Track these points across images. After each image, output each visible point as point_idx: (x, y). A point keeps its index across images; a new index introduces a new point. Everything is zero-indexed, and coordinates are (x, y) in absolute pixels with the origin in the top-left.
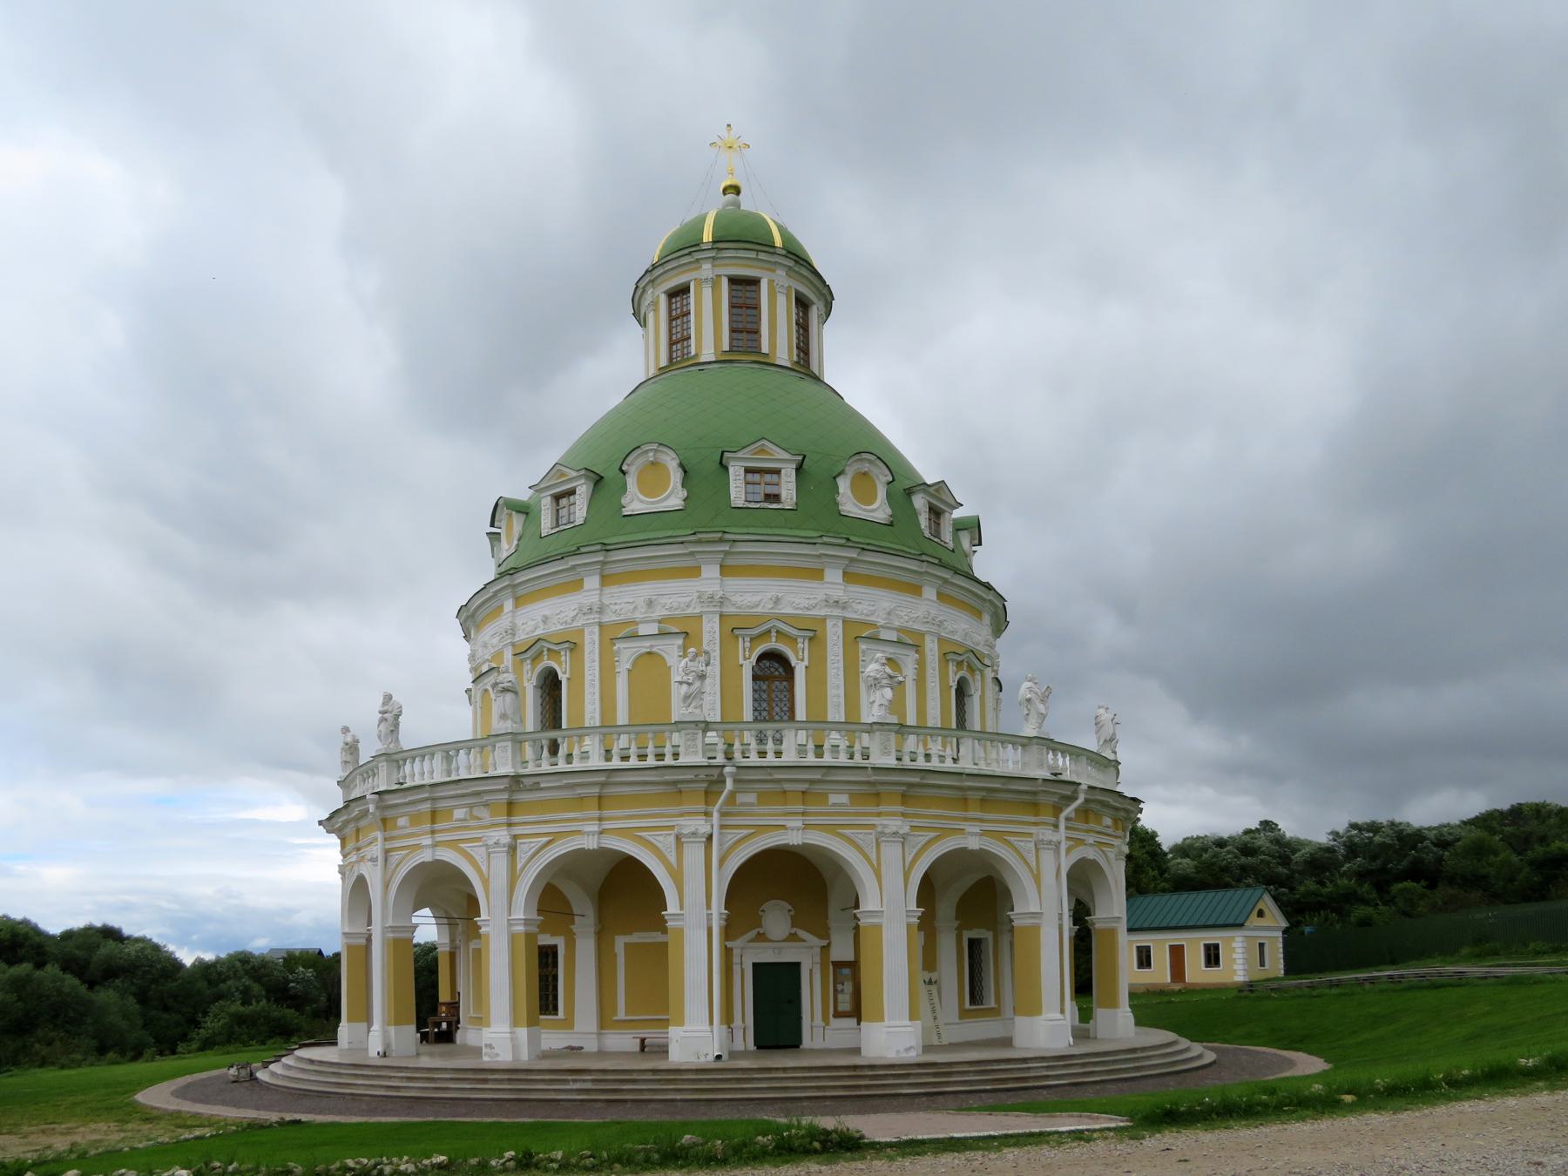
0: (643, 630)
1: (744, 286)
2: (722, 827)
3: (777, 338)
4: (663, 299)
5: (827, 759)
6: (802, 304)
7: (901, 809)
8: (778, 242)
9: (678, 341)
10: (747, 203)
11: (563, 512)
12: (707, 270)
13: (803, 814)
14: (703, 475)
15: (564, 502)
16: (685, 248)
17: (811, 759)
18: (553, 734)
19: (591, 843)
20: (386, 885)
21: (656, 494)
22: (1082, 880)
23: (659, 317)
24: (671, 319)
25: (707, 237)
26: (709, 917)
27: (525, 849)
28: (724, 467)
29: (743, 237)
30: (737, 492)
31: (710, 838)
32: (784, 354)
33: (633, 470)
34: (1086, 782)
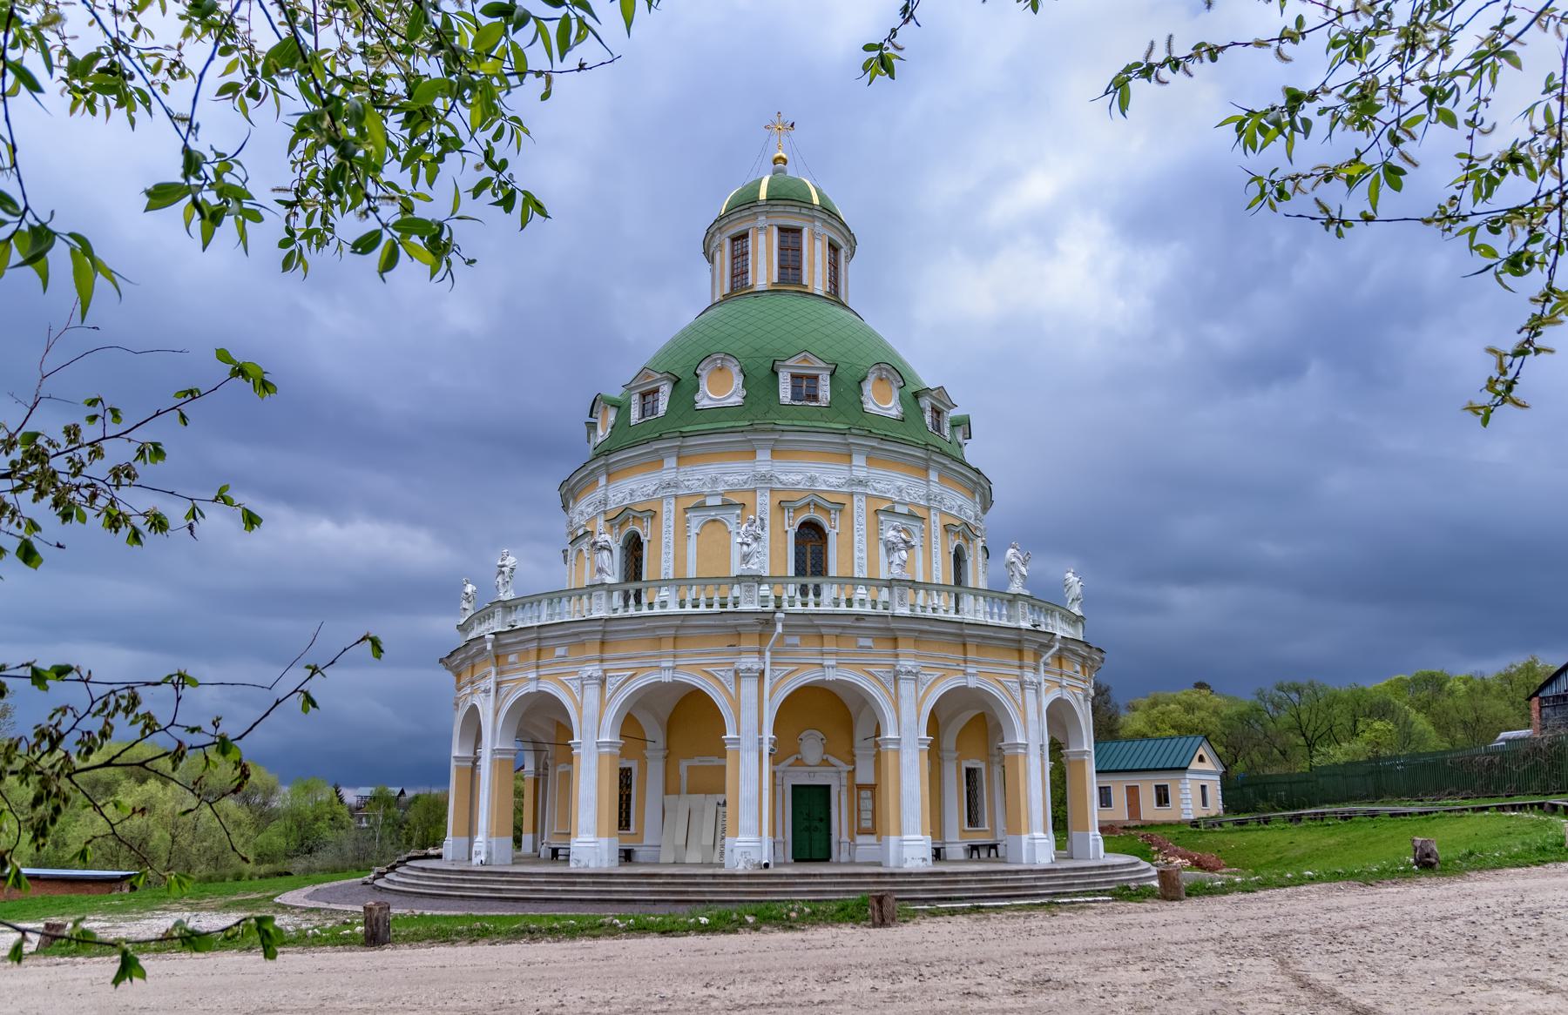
0: (710, 502)
1: (790, 235)
2: (772, 664)
3: (815, 275)
4: (727, 242)
5: (856, 609)
6: (834, 248)
7: (913, 651)
8: (816, 201)
9: (739, 274)
10: (791, 172)
11: (648, 407)
12: (762, 221)
13: (836, 654)
14: (761, 381)
15: (650, 398)
16: (746, 203)
17: (843, 608)
18: (637, 585)
19: (667, 677)
20: (496, 713)
21: (721, 391)
22: (1059, 715)
23: (724, 258)
24: (734, 258)
25: (763, 195)
26: (761, 741)
27: (613, 681)
28: (775, 373)
29: (788, 197)
30: (785, 393)
31: (762, 673)
32: (819, 285)
33: (704, 373)
34: (1059, 634)
